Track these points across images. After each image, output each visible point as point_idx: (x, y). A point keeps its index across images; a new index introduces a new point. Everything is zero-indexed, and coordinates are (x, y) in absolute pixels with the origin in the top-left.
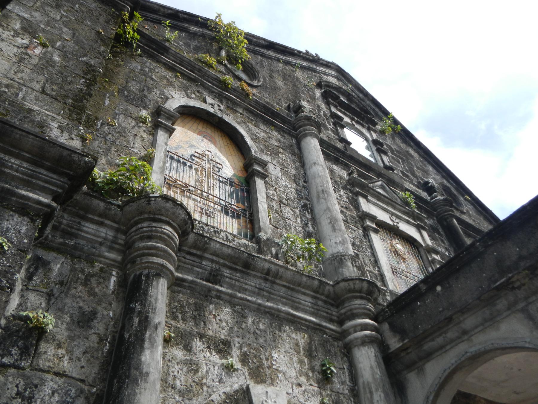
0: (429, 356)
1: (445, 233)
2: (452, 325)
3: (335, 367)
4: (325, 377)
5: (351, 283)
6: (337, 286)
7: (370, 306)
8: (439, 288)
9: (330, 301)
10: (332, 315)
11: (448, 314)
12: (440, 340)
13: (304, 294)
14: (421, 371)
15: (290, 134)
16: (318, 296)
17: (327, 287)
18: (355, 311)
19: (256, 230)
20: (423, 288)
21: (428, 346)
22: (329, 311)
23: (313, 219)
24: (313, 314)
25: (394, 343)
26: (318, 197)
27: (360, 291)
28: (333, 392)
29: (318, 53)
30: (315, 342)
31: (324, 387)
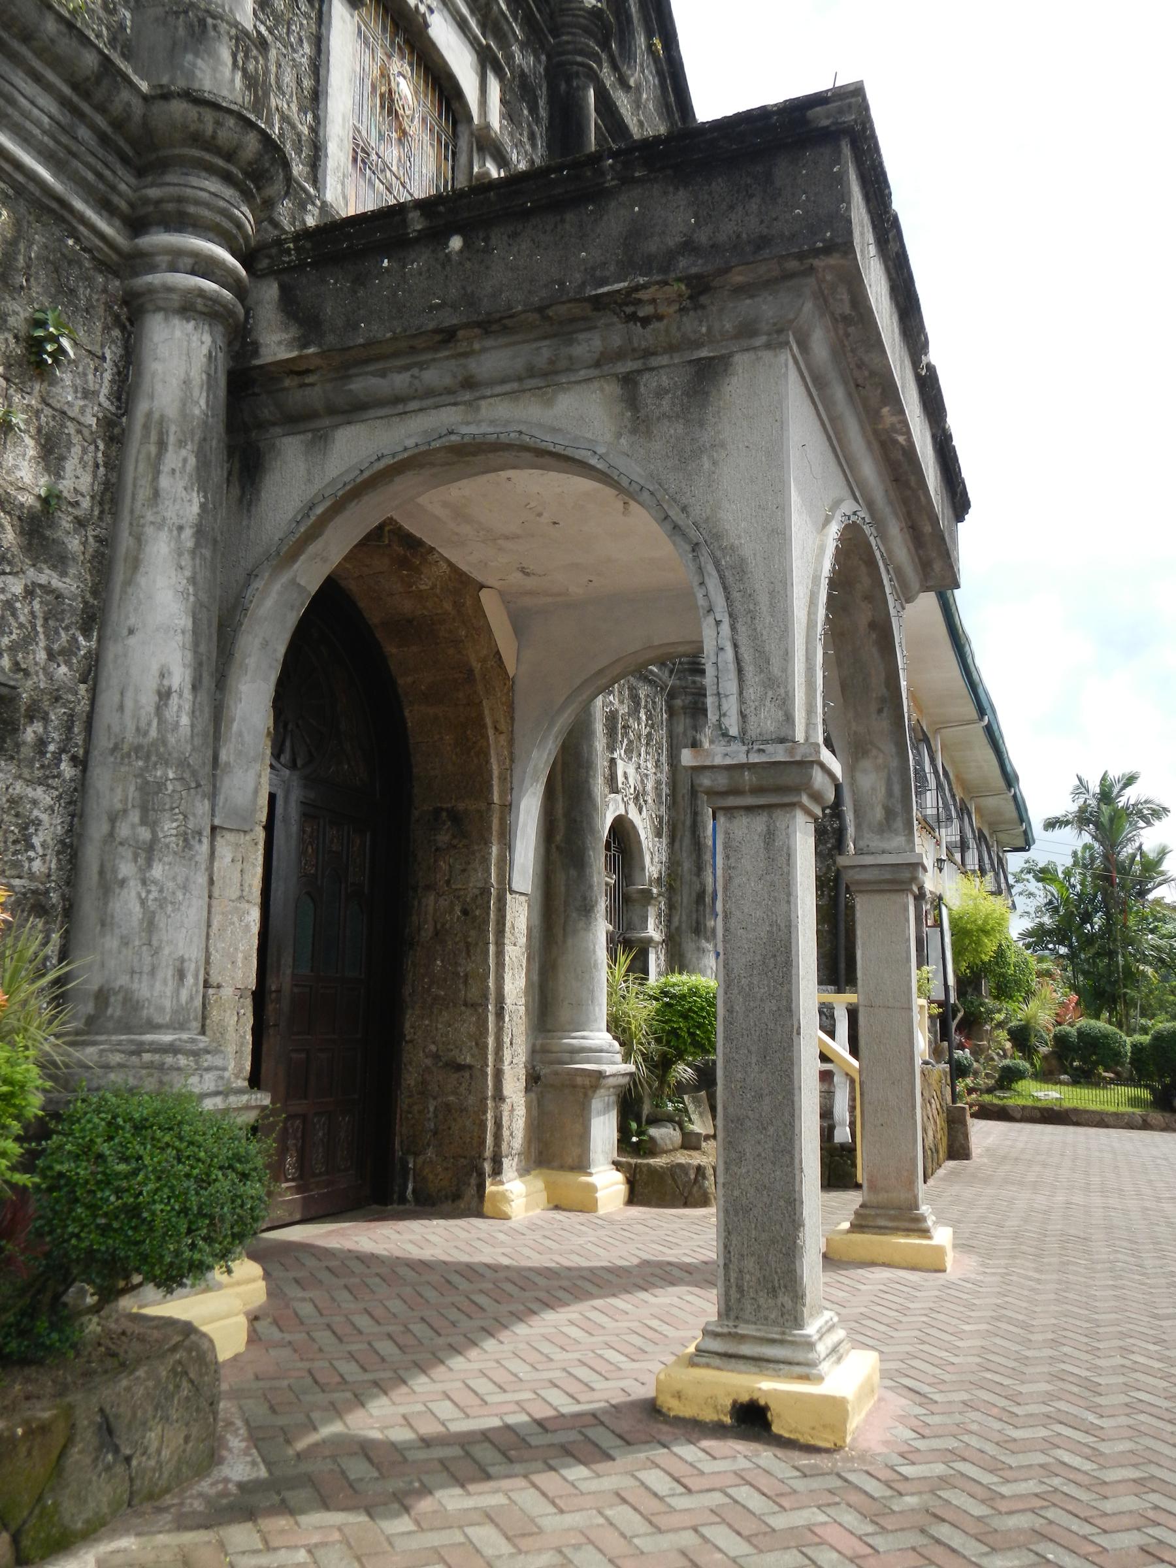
0: (356, 410)
1: (551, 118)
2: (447, 353)
3: (76, 344)
4: (33, 358)
5: (209, 116)
6: (158, 107)
7: (244, 214)
8: (456, 243)
9: (122, 143)
10: (113, 188)
11: (450, 319)
12: (400, 381)
13: (37, 78)
14: (320, 440)
16: (85, 107)
17: (125, 95)
18: (192, 209)
20: (417, 223)
21: (363, 384)
22: (107, 173)
24: (47, 157)
25: (276, 344)
27: (229, 156)
28: (48, 405)
30: (29, 247)
31: (23, 383)
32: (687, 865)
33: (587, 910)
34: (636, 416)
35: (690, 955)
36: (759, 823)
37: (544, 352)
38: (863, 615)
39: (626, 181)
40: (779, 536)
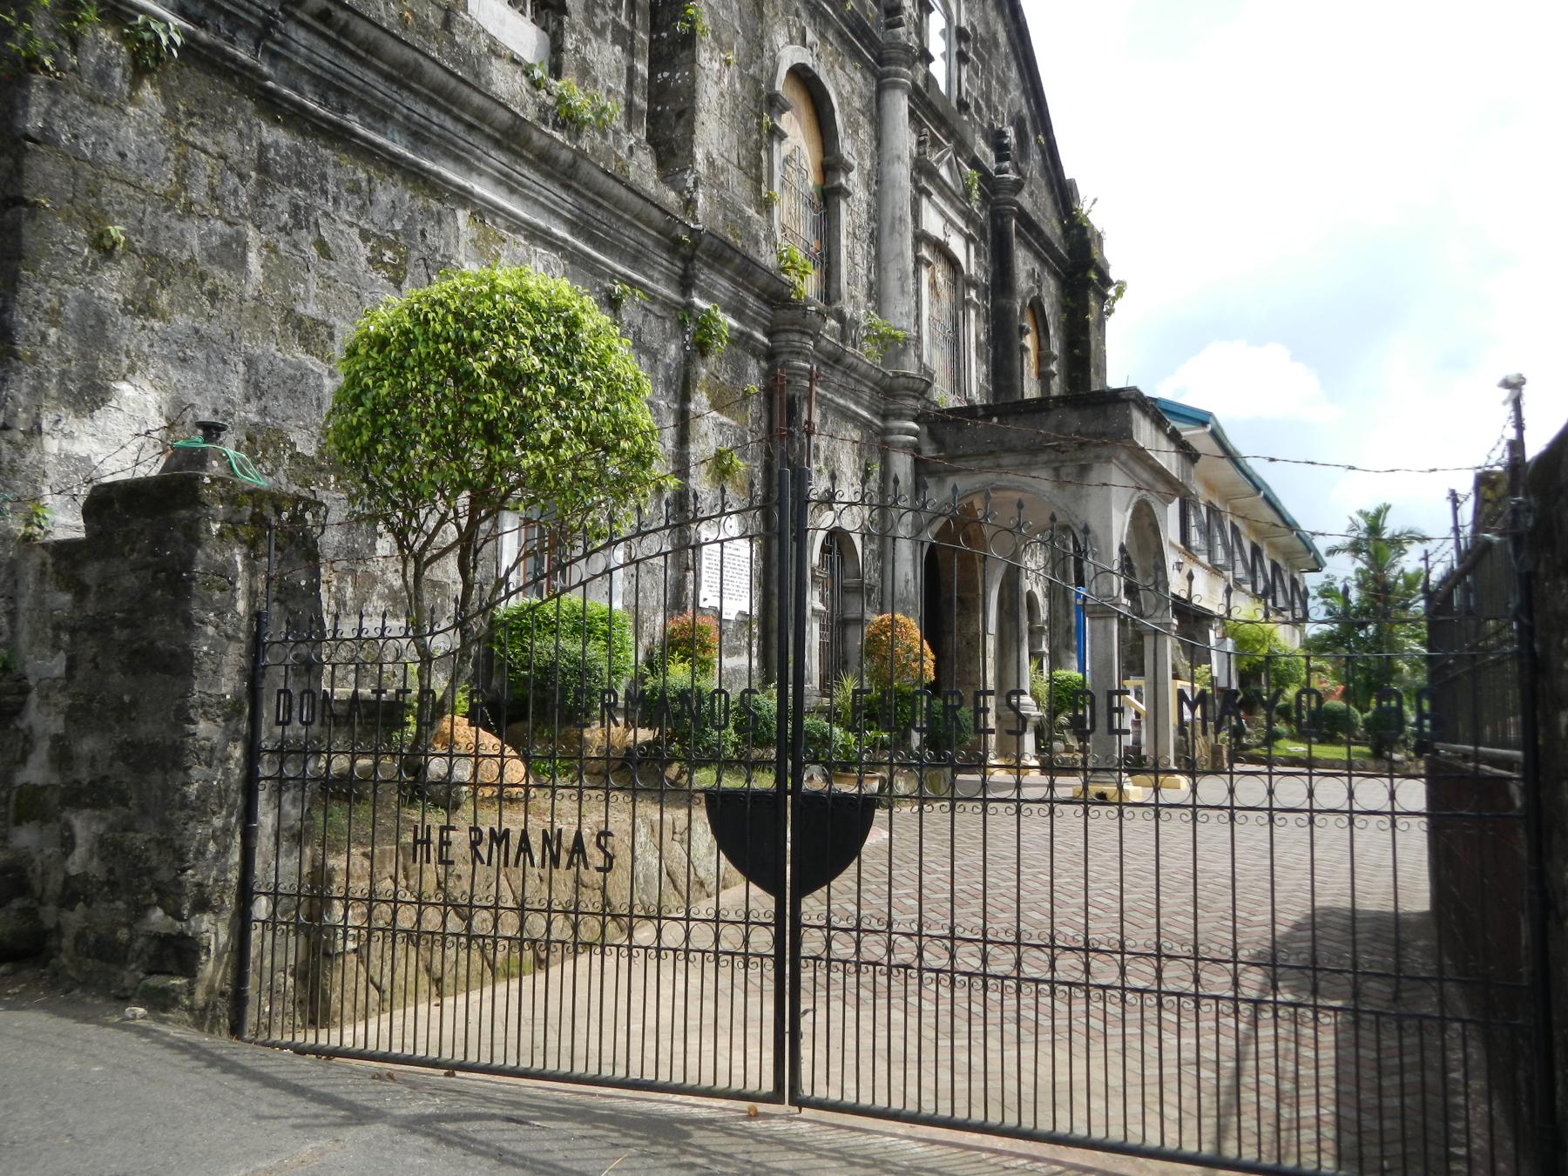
8: (995, 420)
11: (992, 447)
15: (874, 73)
19: (833, 293)
20: (981, 412)
23: (878, 257)
24: (867, 409)
25: (928, 451)
26: (893, 227)
32: (1062, 612)
34: (1059, 482)
35: (1064, 660)
36: (1102, 623)
37: (1027, 459)
38: (1147, 521)
39: (1057, 407)
40: (1108, 527)
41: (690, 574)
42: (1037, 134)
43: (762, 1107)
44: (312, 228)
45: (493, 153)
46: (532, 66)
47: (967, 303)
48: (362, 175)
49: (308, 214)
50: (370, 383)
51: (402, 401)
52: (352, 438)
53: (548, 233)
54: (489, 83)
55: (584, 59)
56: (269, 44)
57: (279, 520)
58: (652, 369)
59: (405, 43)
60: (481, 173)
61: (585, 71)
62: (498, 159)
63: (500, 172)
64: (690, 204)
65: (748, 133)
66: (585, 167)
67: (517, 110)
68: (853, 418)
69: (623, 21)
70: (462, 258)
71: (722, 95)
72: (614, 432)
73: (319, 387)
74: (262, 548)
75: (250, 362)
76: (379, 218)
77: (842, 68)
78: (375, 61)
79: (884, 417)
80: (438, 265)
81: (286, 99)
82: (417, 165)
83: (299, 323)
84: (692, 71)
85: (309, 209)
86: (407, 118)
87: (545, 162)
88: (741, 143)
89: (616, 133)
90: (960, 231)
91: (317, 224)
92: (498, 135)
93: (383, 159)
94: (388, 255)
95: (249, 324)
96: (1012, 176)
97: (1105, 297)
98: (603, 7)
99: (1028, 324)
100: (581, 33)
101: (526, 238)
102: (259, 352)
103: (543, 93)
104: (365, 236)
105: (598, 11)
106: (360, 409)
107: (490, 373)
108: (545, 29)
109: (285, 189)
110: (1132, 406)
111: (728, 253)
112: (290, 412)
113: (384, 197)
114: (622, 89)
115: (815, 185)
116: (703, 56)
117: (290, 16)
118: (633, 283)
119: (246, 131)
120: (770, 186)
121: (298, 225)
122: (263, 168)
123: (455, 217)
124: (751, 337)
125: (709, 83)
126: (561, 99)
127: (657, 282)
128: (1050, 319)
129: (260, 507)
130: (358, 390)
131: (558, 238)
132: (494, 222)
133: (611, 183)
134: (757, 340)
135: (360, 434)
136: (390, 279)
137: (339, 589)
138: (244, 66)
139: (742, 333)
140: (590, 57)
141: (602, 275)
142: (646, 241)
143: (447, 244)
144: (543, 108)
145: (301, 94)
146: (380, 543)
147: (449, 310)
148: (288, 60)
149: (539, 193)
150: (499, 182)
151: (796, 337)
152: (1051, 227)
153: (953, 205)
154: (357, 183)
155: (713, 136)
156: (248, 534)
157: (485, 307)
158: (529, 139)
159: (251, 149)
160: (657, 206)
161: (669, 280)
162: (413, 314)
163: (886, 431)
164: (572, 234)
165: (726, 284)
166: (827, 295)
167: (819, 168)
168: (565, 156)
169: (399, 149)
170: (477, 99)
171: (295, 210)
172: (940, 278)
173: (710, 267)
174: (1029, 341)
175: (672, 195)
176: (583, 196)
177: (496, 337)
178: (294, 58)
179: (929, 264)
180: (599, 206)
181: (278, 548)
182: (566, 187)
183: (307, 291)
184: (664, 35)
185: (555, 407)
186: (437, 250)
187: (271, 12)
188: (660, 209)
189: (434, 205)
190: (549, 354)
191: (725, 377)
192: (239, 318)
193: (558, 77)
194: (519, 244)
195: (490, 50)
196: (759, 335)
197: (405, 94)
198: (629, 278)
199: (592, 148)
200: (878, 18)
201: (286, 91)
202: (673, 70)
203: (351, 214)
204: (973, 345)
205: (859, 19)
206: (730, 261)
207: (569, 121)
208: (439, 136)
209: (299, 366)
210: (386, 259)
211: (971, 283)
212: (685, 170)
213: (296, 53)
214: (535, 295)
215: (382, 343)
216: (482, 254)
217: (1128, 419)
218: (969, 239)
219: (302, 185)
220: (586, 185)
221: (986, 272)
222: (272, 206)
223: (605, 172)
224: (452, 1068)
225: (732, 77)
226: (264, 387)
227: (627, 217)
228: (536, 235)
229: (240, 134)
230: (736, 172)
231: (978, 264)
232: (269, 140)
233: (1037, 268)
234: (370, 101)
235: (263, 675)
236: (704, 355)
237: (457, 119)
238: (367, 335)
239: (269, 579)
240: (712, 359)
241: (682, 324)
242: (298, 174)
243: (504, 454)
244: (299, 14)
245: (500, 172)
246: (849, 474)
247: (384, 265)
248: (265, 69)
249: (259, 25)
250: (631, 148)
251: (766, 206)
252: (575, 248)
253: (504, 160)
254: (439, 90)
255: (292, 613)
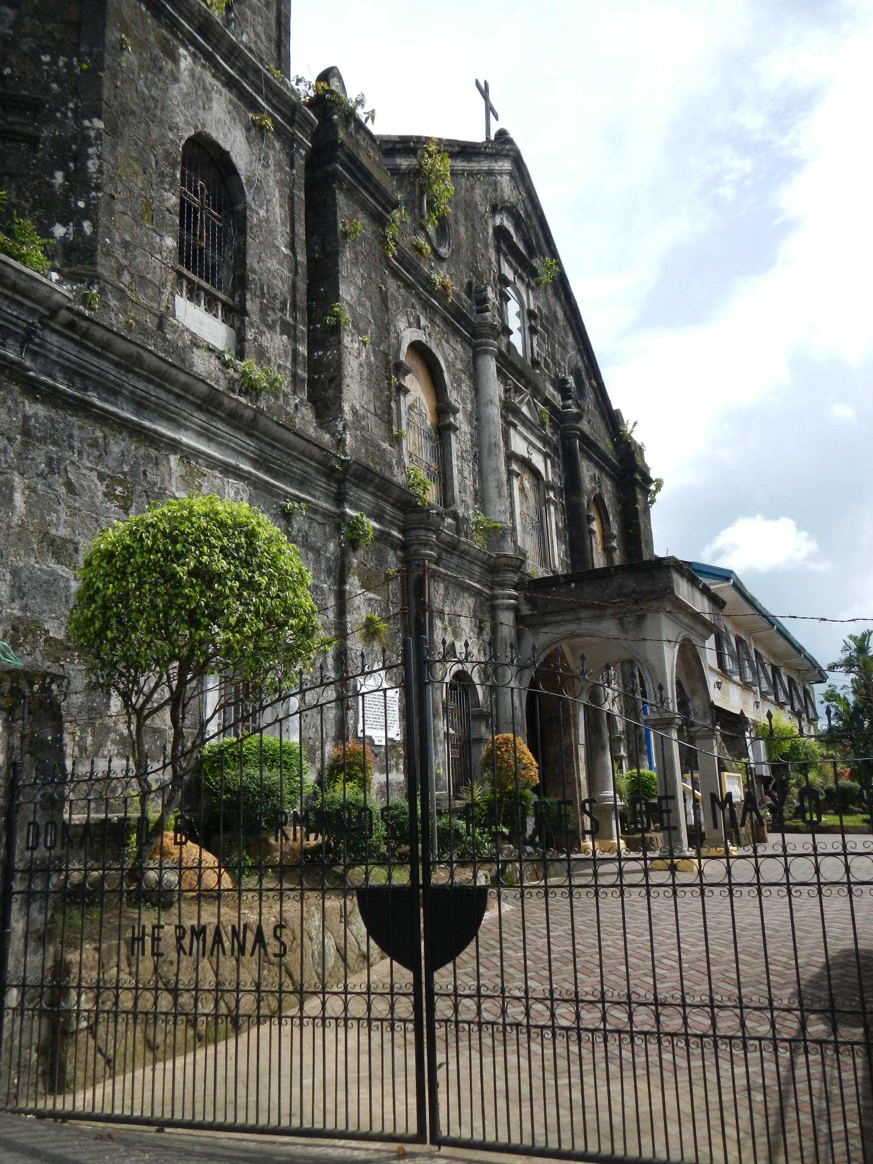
8: (573, 585)
12: (559, 618)
14: (536, 633)
19: (449, 499)
20: (562, 580)
21: (548, 618)
23: (480, 472)
25: (525, 610)
26: (490, 448)
29: (489, 82)
33: (603, 748)
34: (625, 631)
37: (598, 613)
38: (690, 654)
40: (662, 660)
41: (351, 713)
42: (590, 380)
43: (409, 1148)
44: (62, 473)
45: (195, 414)
46: (223, 352)
47: (548, 501)
48: (99, 434)
49: (59, 463)
50: (101, 586)
51: (124, 598)
52: (88, 627)
53: (237, 468)
54: (192, 365)
55: (260, 345)
56: (31, 346)
57: (32, 692)
58: (317, 562)
59: (130, 341)
60: (187, 428)
61: (261, 354)
62: (199, 418)
63: (201, 427)
64: (341, 442)
65: (381, 390)
66: (263, 421)
67: (212, 383)
68: (469, 589)
69: (288, 318)
70: (173, 489)
71: (361, 365)
72: (284, 612)
73: (67, 588)
74: (18, 713)
75: (15, 572)
76: (112, 463)
77: (447, 342)
78: (108, 354)
79: (491, 588)
80: (158, 495)
81: (43, 383)
82: (140, 425)
83: (52, 541)
84: (339, 350)
85: (60, 460)
86: (132, 392)
87: (234, 418)
88: (376, 397)
89: (286, 395)
90: (539, 450)
91: (66, 471)
92: (199, 402)
93: (115, 422)
94: (119, 490)
95: (15, 545)
96: (574, 410)
97: (648, 491)
98: (273, 309)
99: (593, 513)
100: (258, 328)
101: (221, 473)
102: (21, 564)
103: (231, 371)
104: (101, 477)
105: (270, 312)
106: (93, 606)
107: (190, 573)
108: (232, 326)
109: (42, 447)
110: (672, 570)
111: (370, 476)
112: (45, 607)
113: (115, 449)
114: (288, 365)
115: (432, 424)
116: (347, 340)
117: (46, 326)
118: (299, 500)
119: (13, 407)
120: (399, 426)
121: (52, 472)
122: (26, 432)
123: (168, 460)
124: (389, 534)
125: (351, 357)
126: (244, 374)
127: (318, 498)
128: (610, 509)
129: (17, 683)
130: (92, 592)
131: (244, 471)
132: (197, 463)
133: (282, 430)
134: (394, 537)
135: (94, 623)
136: (120, 507)
137: (81, 738)
138: (12, 362)
139: (382, 532)
140: (265, 344)
141: (278, 496)
142: (309, 470)
143: (163, 480)
144: (231, 381)
145: (54, 379)
146: (112, 703)
147: (159, 530)
148: (45, 356)
149: (230, 440)
150: (200, 435)
151: (423, 532)
152: (605, 444)
153: (533, 433)
154: (96, 440)
155: (355, 394)
156: (7, 703)
157: (186, 527)
158: (221, 404)
159: (17, 420)
160: (316, 445)
161: (327, 497)
162: (132, 533)
163: (494, 597)
164: (255, 468)
165: (369, 497)
166: (445, 501)
167: (434, 412)
168: (248, 414)
169: (126, 415)
170: (183, 378)
171: (50, 461)
172: (527, 485)
173: (357, 486)
174: (595, 526)
175: (327, 437)
176: (262, 441)
177: (193, 548)
178: (49, 354)
179: (518, 475)
180: (274, 447)
181: (30, 712)
182: (250, 435)
183: (58, 518)
184: (318, 326)
185: (239, 597)
186: (155, 484)
187: (32, 324)
188: (319, 447)
189: (153, 452)
190: (234, 558)
191: (371, 565)
192: (7, 540)
193: (242, 360)
194: (216, 477)
195: (192, 342)
196: (395, 533)
197: (130, 376)
198: (297, 497)
199: (268, 407)
200: (471, 307)
201: (43, 378)
202: (325, 350)
203: (91, 462)
204: (554, 531)
205: (457, 308)
206: (371, 481)
207: (250, 389)
208: (156, 404)
209: (53, 573)
210: (117, 493)
211: (549, 487)
212: (336, 419)
213: (51, 351)
214: (223, 516)
215: (109, 556)
216: (189, 486)
217: (670, 580)
218: (546, 456)
219: (55, 443)
220: (265, 433)
221: (560, 478)
222: (33, 459)
223: (277, 423)
224: (162, 1125)
225: (368, 353)
226: (26, 590)
227: (294, 454)
228: (228, 470)
229: (9, 409)
230: (373, 418)
231: (554, 473)
232: (31, 413)
233: (597, 473)
234: (105, 382)
235: (17, 812)
236: (355, 549)
237: (169, 391)
238: (99, 551)
239: (23, 737)
240: (361, 552)
241: (338, 528)
242: (52, 436)
243: (202, 633)
244: (52, 324)
245: (201, 427)
246: (468, 630)
247: (116, 497)
248: (28, 364)
249: (23, 333)
250: (296, 405)
251: (396, 440)
252: (257, 477)
253: (204, 419)
254: (155, 372)
255: (41, 762)
